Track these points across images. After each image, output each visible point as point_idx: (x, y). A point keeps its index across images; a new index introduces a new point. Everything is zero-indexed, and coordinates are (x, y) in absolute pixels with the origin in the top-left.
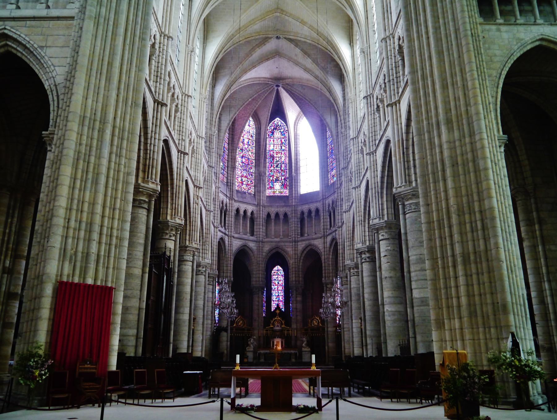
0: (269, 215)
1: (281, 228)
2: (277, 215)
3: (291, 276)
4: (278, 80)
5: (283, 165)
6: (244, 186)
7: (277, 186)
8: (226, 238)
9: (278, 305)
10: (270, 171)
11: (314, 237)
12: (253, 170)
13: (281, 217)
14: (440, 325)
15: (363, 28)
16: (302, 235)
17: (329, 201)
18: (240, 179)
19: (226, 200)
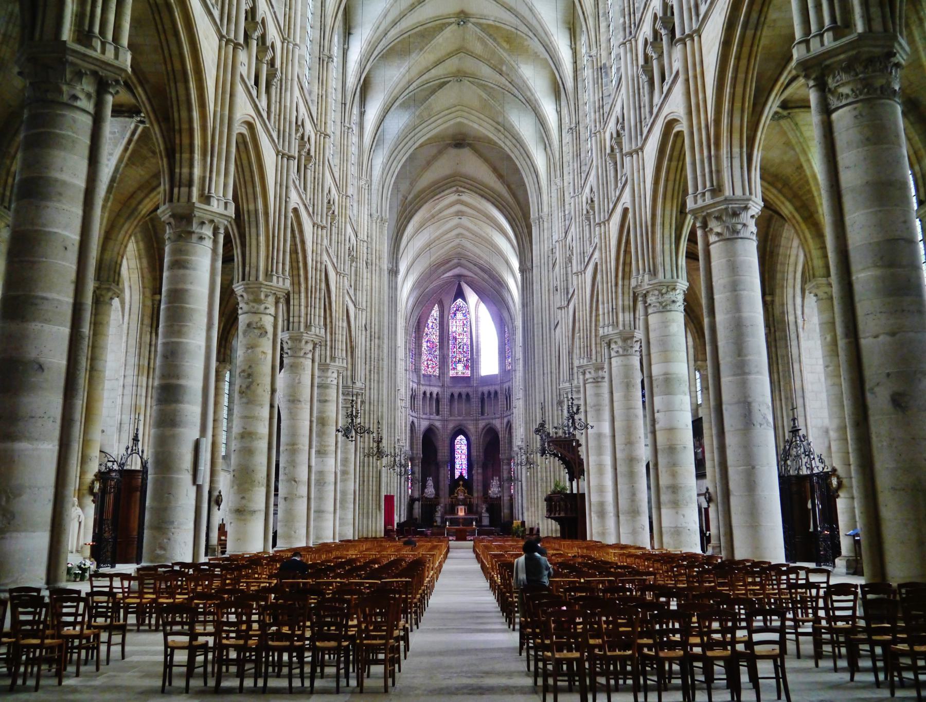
0: (452, 395)
1: (463, 406)
2: (460, 395)
3: (472, 451)
4: (459, 276)
5: (465, 347)
6: (430, 369)
7: (460, 367)
8: (415, 420)
9: (461, 473)
10: (453, 352)
11: (493, 416)
12: (437, 353)
13: (464, 397)
14: (528, 509)
15: (571, 97)
16: (483, 414)
17: (506, 386)
18: (425, 363)
19: (415, 386)
